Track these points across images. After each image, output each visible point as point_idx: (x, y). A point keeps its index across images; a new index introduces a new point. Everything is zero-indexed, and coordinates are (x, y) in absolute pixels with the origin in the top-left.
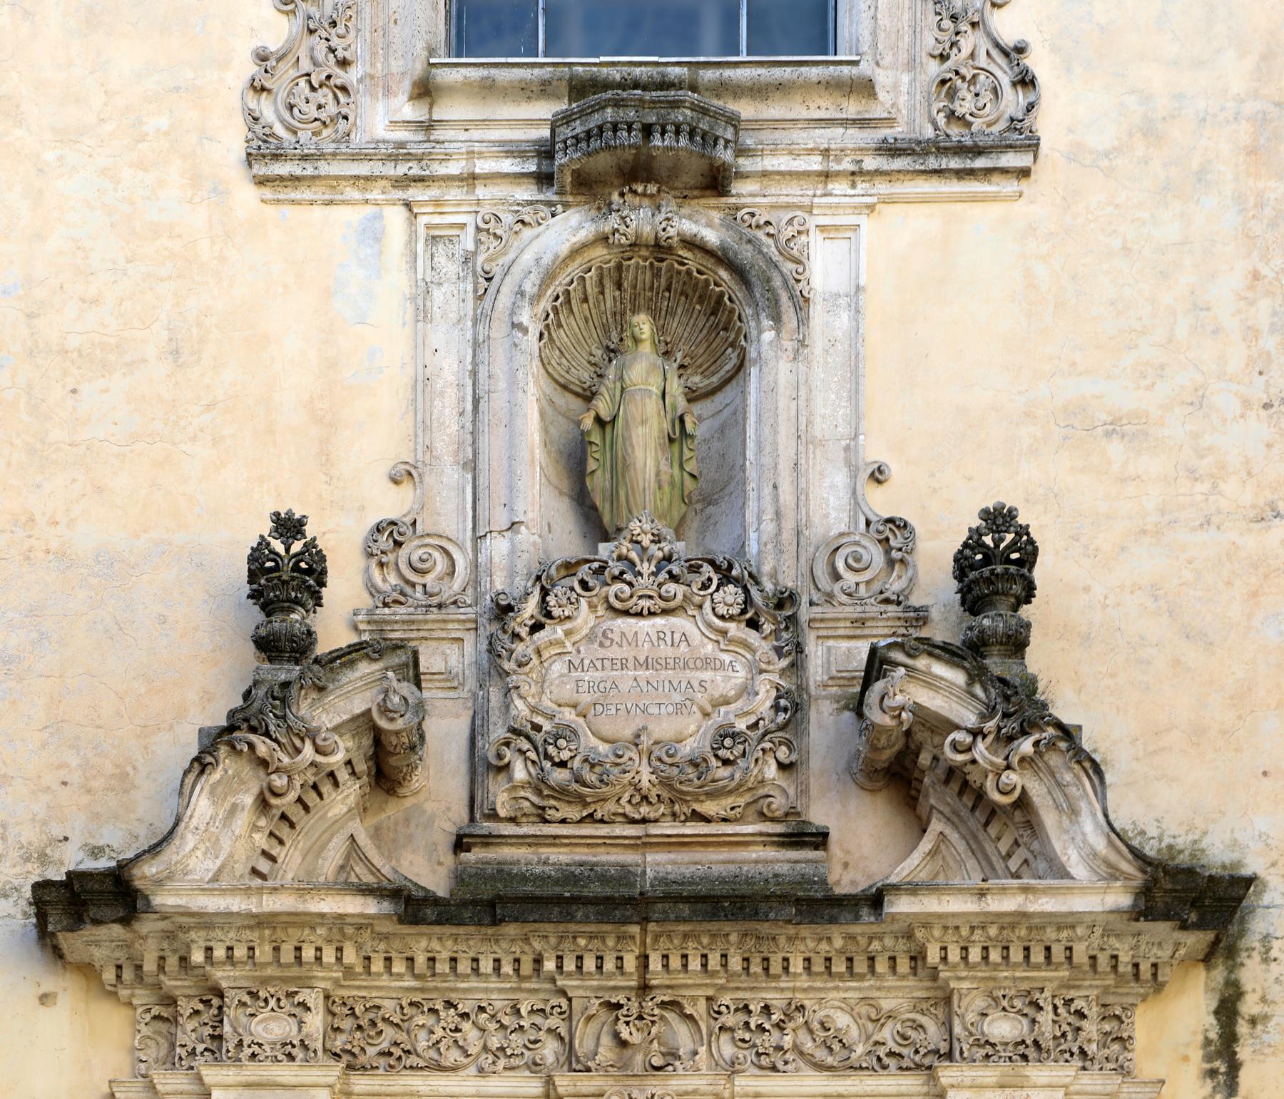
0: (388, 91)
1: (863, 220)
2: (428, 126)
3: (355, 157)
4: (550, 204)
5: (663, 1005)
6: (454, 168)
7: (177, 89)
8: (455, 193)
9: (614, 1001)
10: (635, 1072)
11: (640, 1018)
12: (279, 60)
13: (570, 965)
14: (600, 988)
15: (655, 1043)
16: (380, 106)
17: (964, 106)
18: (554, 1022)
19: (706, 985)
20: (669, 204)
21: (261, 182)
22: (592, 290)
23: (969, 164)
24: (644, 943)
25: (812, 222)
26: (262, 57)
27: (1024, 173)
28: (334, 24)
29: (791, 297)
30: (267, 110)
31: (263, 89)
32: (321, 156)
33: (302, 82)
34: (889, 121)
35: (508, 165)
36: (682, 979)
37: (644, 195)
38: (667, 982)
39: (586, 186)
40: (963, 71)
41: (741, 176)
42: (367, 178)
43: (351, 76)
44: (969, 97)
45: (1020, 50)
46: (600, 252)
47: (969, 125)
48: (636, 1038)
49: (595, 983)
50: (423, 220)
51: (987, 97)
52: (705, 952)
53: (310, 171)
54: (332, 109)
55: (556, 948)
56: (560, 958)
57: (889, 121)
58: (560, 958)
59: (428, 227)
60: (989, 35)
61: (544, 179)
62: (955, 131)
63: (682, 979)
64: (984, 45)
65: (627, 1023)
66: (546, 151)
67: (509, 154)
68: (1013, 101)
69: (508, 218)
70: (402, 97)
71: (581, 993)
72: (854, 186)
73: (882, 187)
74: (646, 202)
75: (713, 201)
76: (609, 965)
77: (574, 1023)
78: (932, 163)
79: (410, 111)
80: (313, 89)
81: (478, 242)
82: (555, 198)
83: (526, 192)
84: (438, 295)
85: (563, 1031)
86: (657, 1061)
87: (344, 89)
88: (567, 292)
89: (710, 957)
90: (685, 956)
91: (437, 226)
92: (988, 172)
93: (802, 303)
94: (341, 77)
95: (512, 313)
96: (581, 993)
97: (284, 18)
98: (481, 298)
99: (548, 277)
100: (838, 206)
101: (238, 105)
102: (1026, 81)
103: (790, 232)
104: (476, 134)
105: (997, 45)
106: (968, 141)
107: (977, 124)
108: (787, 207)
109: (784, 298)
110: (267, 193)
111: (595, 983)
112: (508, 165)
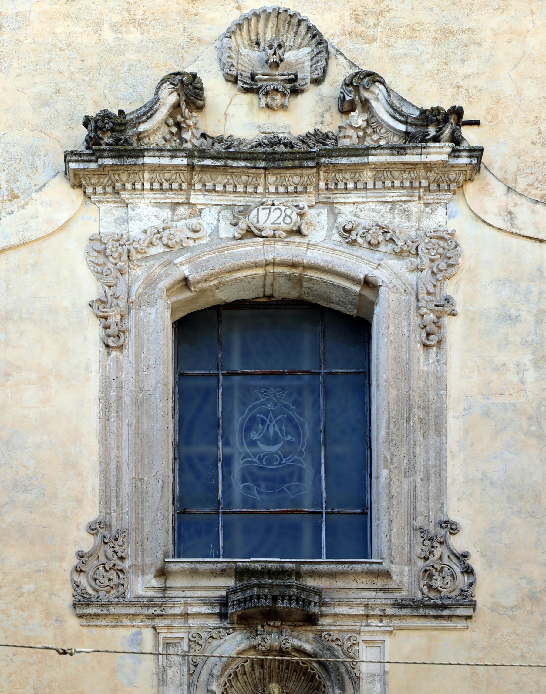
0: (144, 573)
1: (387, 638)
2: (164, 589)
3: (127, 605)
4: (226, 628)
6: (178, 610)
7: (39, 571)
8: (178, 622)
12: (89, 557)
16: (140, 579)
17: (437, 583)
20: (287, 630)
21: (80, 616)
22: (248, 669)
23: (440, 613)
25: (360, 639)
26: (80, 555)
27: (469, 617)
28: (117, 540)
29: (350, 678)
30: (83, 580)
31: (81, 571)
32: (111, 605)
33: (101, 568)
34: (399, 590)
35: (204, 609)
37: (274, 626)
39: (245, 621)
40: (436, 566)
41: (323, 615)
42: (133, 615)
43: (126, 565)
44: (439, 579)
45: (465, 556)
46: (252, 655)
47: (440, 592)
50: (162, 635)
51: (449, 579)
53: (105, 612)
54: (116, 580)
57: (399, 590)
59: (165, 639)
60: (449, 548)
61: (223, 616)
62: (432, 595)
64: (446, 553)
66: (224, 603)
67: (205, 604)
68: (462, 581)
69: (205, 635)
70: (151, 576)
72: (381, 621)
73: (396, 622)
74: (275, 630)
75: (309, 628)
78: (421, 612)
79: (154, 582)
80: (106, 570)
81: (189, 647)
82: (229, 626)
83: (213, 623)
84: (170, 672)
87: (121, 571)
88: (235, 673)
91: (169, 639)
92: (450, 617)
93: (356, 680)
94: (121, 565)
95: (208, 684)
97: (92, 537)
98: (191, 675)
99: (226, 666)
100: (373, 632)
101: (69, 578)
102: (468, 571)
103: (349, 644)
104: (188, 593)
105: (453, 553)
106: (439, 602)
107: (444, 592)
108: (347, 631)
109: (346, 678)
110: (84, 621)
112: (204, 609)
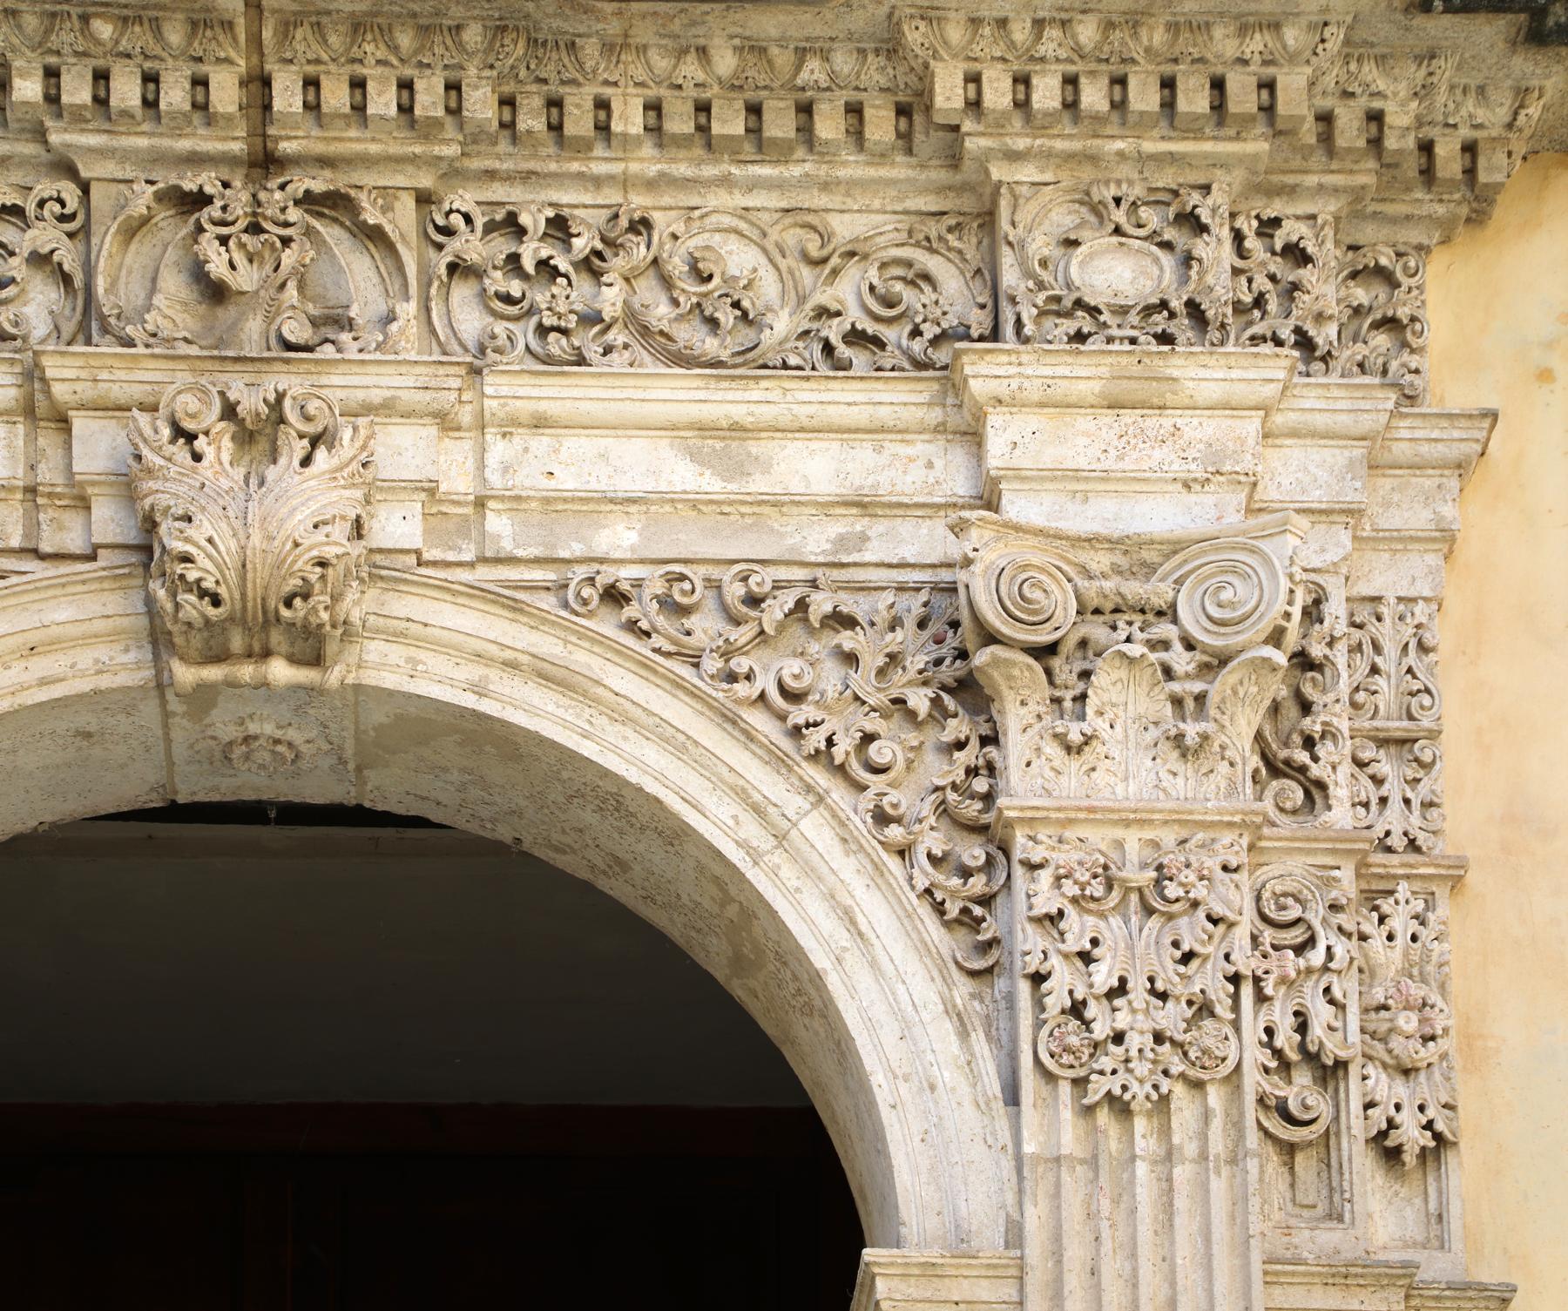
5: (308, 200)
9: (189, 185)
10: (246, 353)
11: (255, 229)
13: (77, 91)
14: (159, 158)
15: (292, 291)
18: (46, 236)
19: (413, 159)
24: (256, 42)
36: (353, 142)
38: (320, 148)
48: (245, 278)
49: (143, 142)
52: (408, 72)
55: (40, 46)
56: (52, 74)
58: (52, 74)
63: (353, 142)
65: (224, 240)
71: (109, 169)
76: (175, 95)
77: (95, 241)
85: (68, 256)
86: (296, 330)
89: (419, 85)
90: (358, 84)
96: (109, 169)
111: (143, 142)
